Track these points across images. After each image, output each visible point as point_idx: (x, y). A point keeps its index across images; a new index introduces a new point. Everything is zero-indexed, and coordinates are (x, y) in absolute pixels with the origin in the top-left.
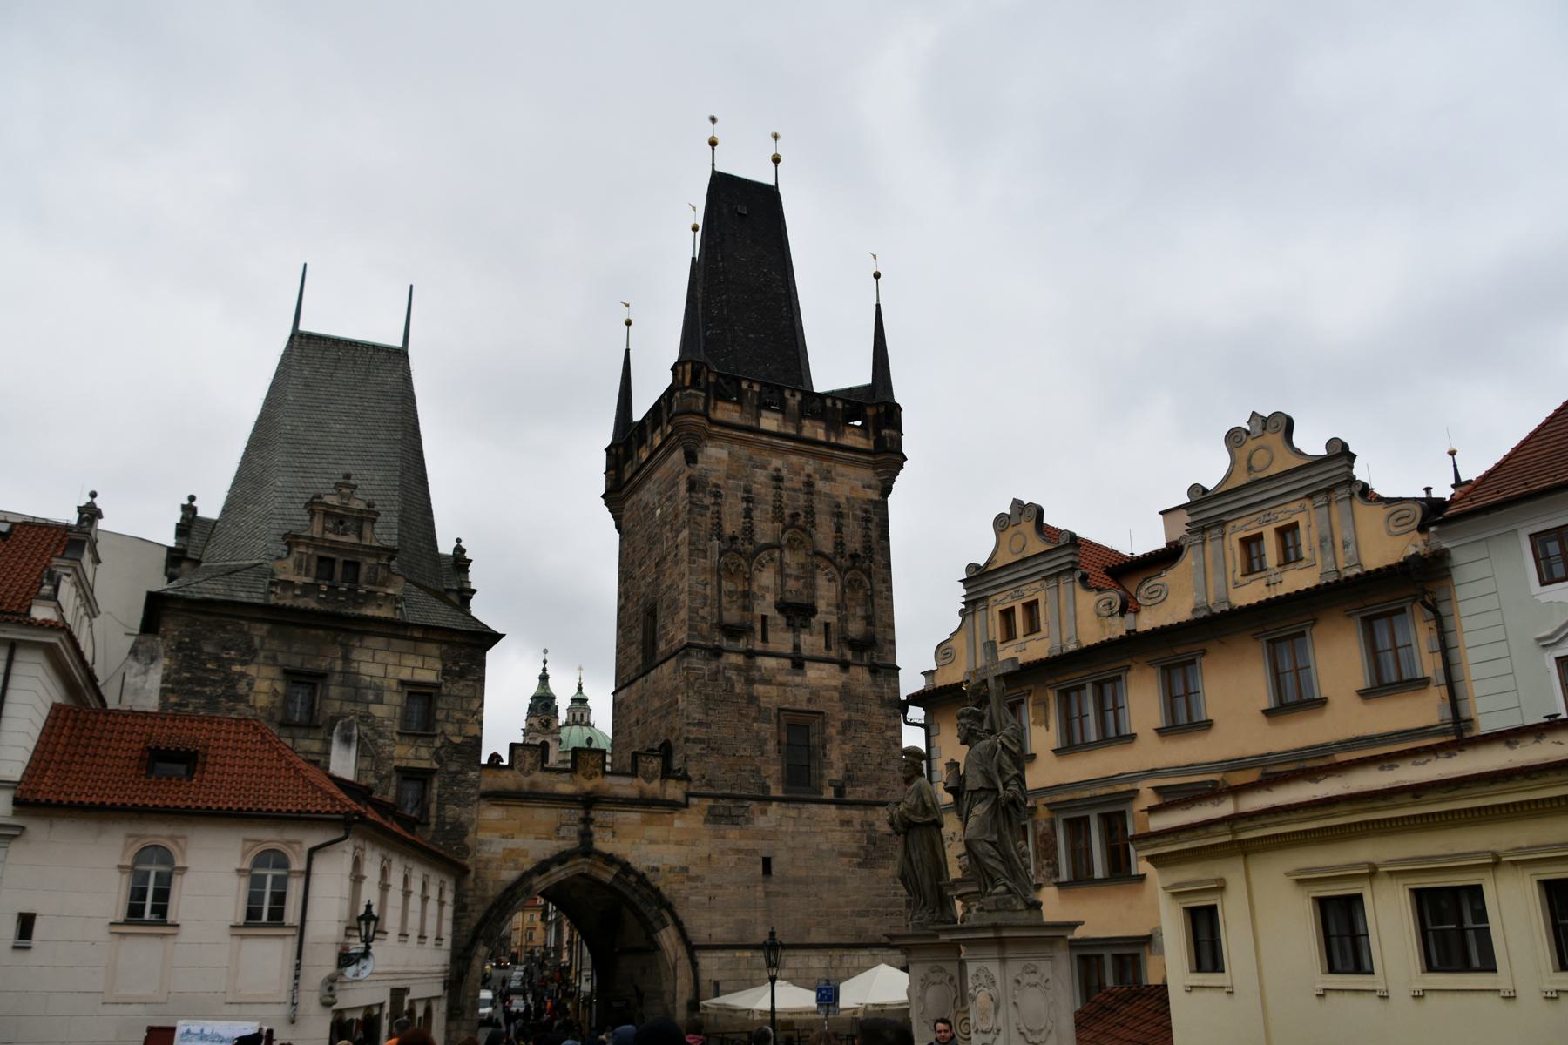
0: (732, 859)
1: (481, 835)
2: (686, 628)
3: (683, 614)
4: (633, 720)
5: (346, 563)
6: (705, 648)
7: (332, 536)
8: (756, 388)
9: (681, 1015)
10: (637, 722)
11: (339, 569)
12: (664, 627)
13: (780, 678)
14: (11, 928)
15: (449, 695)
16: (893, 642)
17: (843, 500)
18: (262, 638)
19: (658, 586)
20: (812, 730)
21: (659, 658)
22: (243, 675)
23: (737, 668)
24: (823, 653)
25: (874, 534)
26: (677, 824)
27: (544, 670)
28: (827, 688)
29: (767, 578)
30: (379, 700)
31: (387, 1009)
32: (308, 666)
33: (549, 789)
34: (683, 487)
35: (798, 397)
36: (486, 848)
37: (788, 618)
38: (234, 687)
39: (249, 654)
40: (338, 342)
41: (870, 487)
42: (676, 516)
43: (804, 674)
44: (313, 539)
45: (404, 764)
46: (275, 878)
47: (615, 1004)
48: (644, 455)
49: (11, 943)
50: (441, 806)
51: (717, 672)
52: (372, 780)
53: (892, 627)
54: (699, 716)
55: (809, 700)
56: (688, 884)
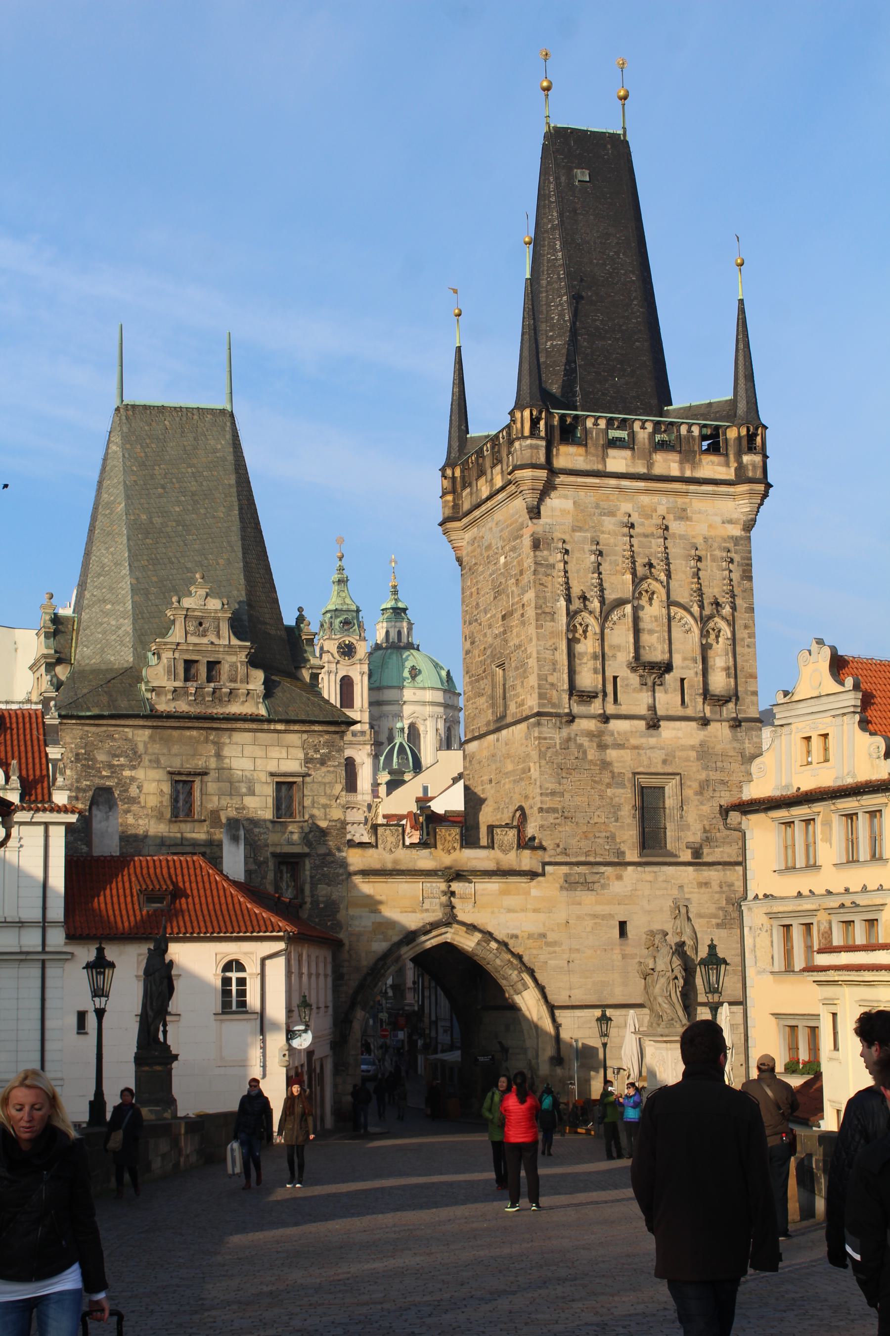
0: (589, 923)
1: (352, 912)
2: (535, 696)
3: (533, 680)
4: (486, 778)
5: (208, 662)
6: (557, 715)
7: (192, 639)
8: (602, 423)
9: (544, 1069)
10: (491, 781)
11: (203, 670)
12: (513, 687)
13: (633, 741)
14: (73, 1020)
15: (313, 782)
16: (755, 693)
17: (699, 541)
18: (145, 744)
19: (506, 641)
20: (668, 791)
21: (509, 719)
22: (133, 779)
23: (590, 735)
24: (680, 712)
25: (736, 576)
26: (534, 892)
27: (341, 569)
28: (683, 748)
29: (620, 635)
30: (252, 792)
31: (306, 1068)
32: (189, 766)
33: (410, 866)
34: (527, 542)
35: (649, 427)
37: (641, 676)
38: (126, 791)
39: (135, 758)
40: (162, 409)
41: (730, 522)
42: (521, 573)
43: (660, 735)
44: (178, 644)
45: (278, 850)
46: (238, 979)
47: (481, 1059)
48: (485, 492)
49: (75, 1030)
50: (314, 886)
51: (569, 739)
52: (253, 867)
53: (753, 676)
54: (551, 786)
55: (664, 762)
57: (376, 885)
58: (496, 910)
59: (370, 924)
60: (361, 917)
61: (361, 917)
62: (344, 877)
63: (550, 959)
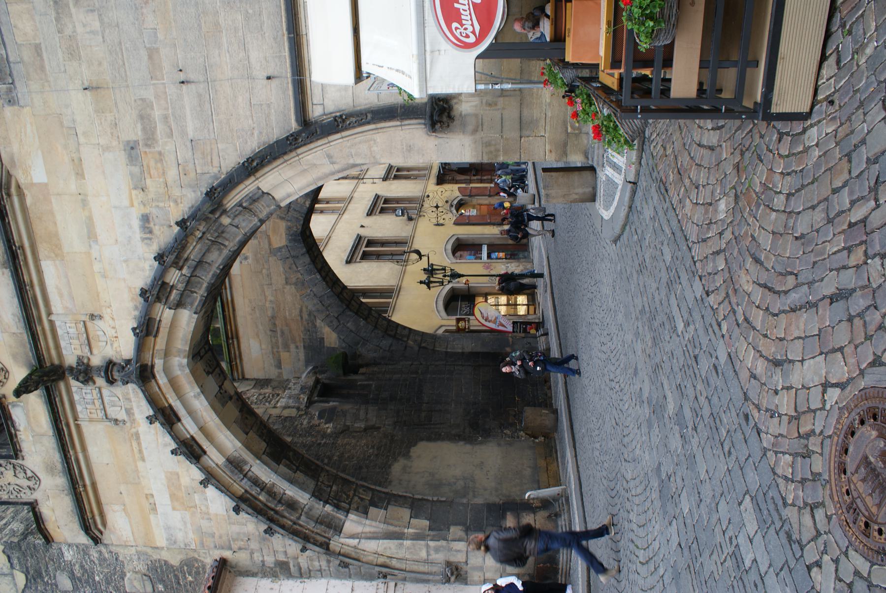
36: (180, 536)
56: (164, 144)
57: (103, 500)
58: (97, 267)
59: (177, 515)
60: (168, 528)
61: (168, 528)
62: (103, 550)
63: (183, 133)
